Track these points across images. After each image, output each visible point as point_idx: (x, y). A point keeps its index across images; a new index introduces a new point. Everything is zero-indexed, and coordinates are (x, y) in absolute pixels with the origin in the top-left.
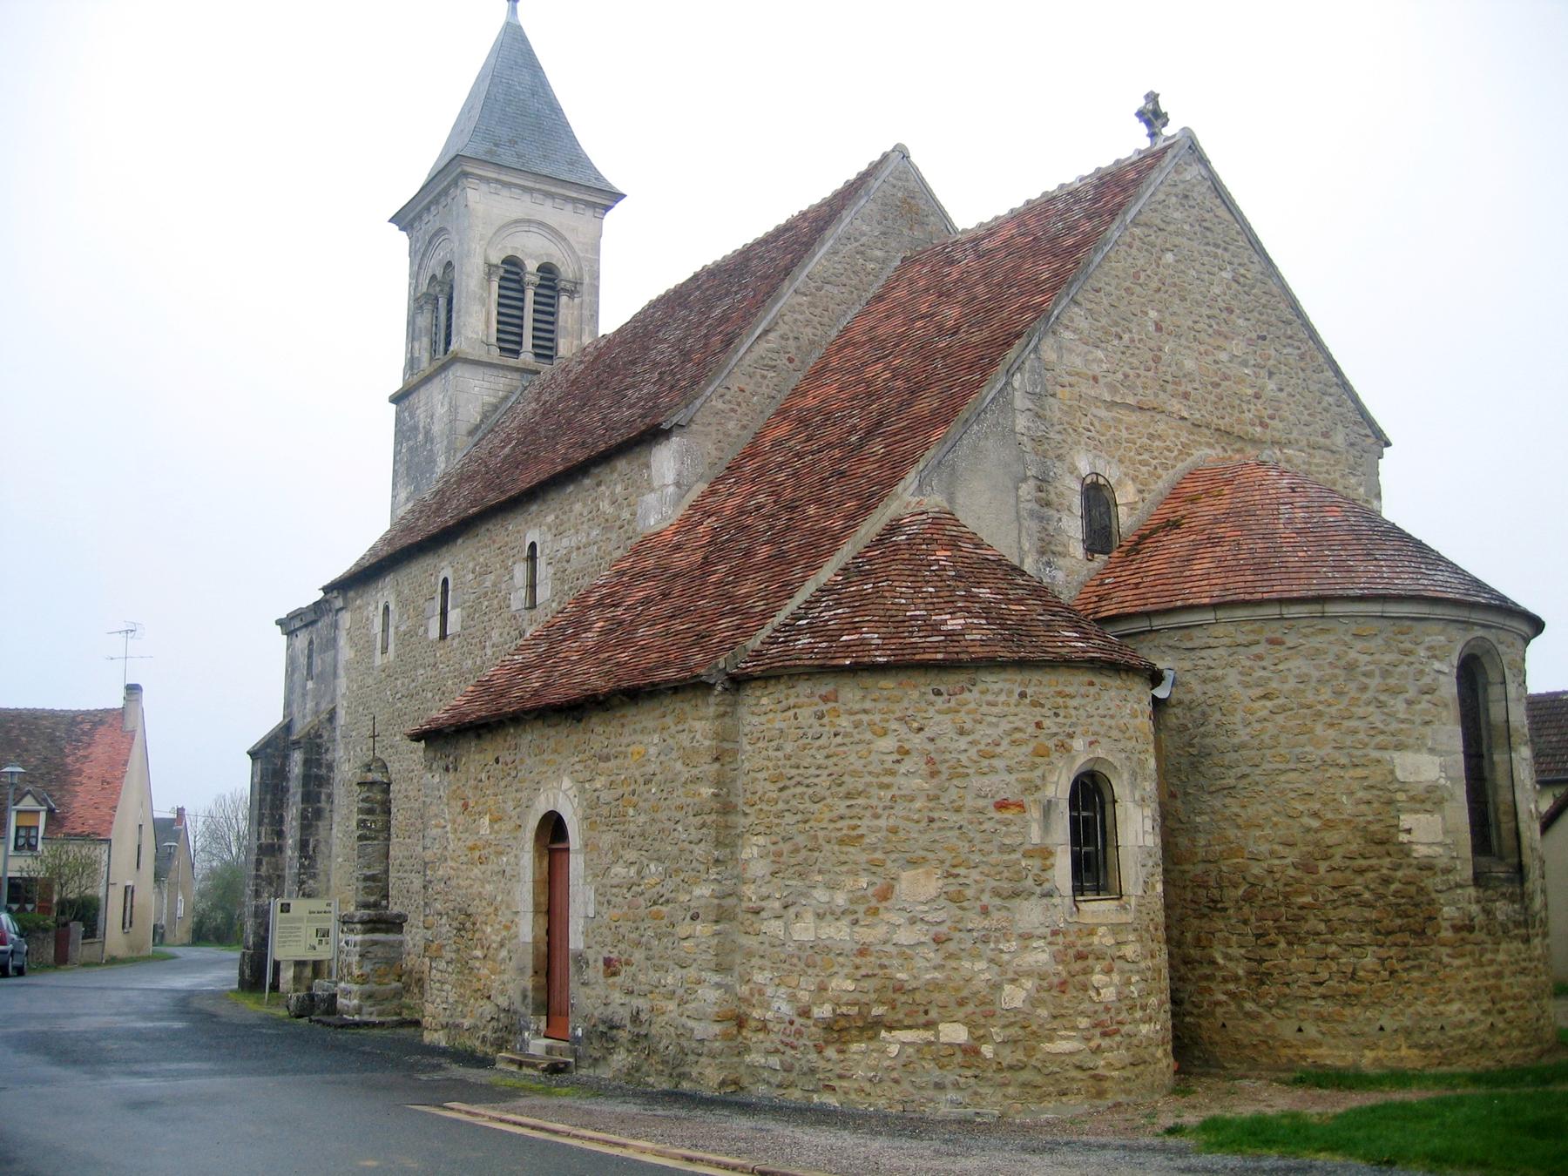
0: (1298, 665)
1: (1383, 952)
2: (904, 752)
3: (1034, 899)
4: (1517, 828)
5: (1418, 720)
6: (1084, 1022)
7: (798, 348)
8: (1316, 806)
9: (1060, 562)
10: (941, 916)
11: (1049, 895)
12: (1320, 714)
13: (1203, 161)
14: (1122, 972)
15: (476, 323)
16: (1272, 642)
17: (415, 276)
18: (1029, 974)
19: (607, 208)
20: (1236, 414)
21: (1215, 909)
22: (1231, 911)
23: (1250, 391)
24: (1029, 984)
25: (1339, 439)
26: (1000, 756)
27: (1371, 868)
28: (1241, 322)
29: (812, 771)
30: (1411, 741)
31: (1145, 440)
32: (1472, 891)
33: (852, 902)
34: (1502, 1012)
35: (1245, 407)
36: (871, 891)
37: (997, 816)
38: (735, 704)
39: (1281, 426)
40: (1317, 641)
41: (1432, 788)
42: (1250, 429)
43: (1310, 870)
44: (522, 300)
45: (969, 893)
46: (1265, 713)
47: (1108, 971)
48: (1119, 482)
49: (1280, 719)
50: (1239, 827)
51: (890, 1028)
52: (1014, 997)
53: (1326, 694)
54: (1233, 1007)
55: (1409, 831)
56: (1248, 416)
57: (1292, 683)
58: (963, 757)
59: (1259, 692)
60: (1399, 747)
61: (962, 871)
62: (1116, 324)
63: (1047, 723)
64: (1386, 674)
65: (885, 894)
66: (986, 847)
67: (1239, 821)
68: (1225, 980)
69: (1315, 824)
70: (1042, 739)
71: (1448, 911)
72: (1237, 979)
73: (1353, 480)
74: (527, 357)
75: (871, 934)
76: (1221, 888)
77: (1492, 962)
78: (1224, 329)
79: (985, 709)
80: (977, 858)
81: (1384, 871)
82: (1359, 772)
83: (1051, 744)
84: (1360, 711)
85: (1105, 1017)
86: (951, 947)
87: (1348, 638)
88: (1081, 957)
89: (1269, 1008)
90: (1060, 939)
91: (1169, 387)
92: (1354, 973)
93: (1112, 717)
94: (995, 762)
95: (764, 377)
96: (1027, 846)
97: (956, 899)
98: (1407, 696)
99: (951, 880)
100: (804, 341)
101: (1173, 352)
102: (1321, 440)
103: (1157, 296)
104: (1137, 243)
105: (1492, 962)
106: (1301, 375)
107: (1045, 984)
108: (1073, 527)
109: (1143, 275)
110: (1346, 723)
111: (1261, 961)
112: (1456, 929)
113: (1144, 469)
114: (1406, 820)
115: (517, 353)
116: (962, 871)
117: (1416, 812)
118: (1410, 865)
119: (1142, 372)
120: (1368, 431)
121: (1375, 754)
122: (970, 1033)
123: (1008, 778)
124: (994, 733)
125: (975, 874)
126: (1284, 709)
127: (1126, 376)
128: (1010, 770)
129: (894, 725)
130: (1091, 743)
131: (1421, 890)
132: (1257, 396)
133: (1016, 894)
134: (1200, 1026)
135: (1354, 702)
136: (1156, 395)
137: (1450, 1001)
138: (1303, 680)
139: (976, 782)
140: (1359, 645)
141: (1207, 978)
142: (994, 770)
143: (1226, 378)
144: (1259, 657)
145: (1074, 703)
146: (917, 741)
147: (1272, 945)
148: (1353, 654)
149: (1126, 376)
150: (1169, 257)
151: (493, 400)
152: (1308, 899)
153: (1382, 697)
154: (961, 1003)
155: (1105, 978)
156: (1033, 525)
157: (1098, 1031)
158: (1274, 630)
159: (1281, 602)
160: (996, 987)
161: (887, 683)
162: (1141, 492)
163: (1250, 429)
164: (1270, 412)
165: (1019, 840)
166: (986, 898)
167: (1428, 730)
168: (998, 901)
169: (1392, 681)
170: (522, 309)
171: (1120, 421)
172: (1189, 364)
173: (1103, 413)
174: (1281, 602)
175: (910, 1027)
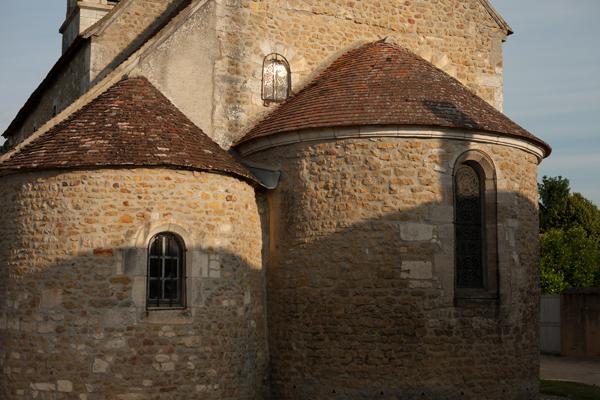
1: (386, 346)
3: (116, 307)
4: (498, 270)
6: (147, 383)
9: (244, 107)
11: (128, 305)
12: (352, 197)
14: (180, 353)
18: (109, 352)
21: (292, 316)
22: (300, 319)
24: (110, 359)
25: (471, 29)
26: (98, 222)
27: (381, 294)
29: (9, 231)
31: (317, 32)
32: (453, 310)
33: (20, 307)
34: (472, 385)
35: (397, 10)
36: (28, 302)
37: (95, 258)
41: (426, 245)
45: (76, 303)
47: (170, 352)
50: (307, 267)
51: (34, 382)
52: (101, 366)
54: (299, 377)
55: (408, 271)
56: (399, 16)
58: (76, 222)
65: (34, 303)
66: (87, 276)
67: (307, 263)
68: (297, 360)
69: (348, 266)
71: (432, 322)
72: (302, 359)
73: (480, 55)
75: (27, 328)
76: (296, 304)
77: (464, 355)
79: (92, 194)
80: (81, 282)
81: (389, 296)
82: (378, 234)
83: (134, 215)
85: (164, 379)
86: (65, 335)
88: (148, 343)
89: (317, 377)
90: (134, 332)
92: (367, 358)
93: (183, 198)
94: (95, 226)
95: (153, 6)
96: (113, 276)
98: (412, 186)
99: (67, 296)
105: (464, 355)
107: (121, 358)
111: (315, 349)
112: (438, 333)
113: (315, 51)
114: (406, 265)
116: (72, 290)
117: (414, 259)
118: (406, 293)
120: (497, 25)
121: (389, 223)
122: (74, 387)
123: (103, 235)
125: (80, 292)
130: (164, 215)
131: (413, 308)
133: (104, 304)
134: (283, 386)
137: (430, 378)
139: (83, 235)
141: (289, 358)
145: (149, 189)
147: (320, 340)
152: (339, 313)
153: (394, 187)
154: (69, 368)
155: (167, 357)
156: (225, 85)
157: (158, 388)
159: (334, 128)
162: (310, 64)
163: (401, 24)
164: (417, 13)
165: (107, 272)
166: (85, 307)
168: (93, 309)
173: (286, 17)
174: (334, 128)
175: (42, 381)
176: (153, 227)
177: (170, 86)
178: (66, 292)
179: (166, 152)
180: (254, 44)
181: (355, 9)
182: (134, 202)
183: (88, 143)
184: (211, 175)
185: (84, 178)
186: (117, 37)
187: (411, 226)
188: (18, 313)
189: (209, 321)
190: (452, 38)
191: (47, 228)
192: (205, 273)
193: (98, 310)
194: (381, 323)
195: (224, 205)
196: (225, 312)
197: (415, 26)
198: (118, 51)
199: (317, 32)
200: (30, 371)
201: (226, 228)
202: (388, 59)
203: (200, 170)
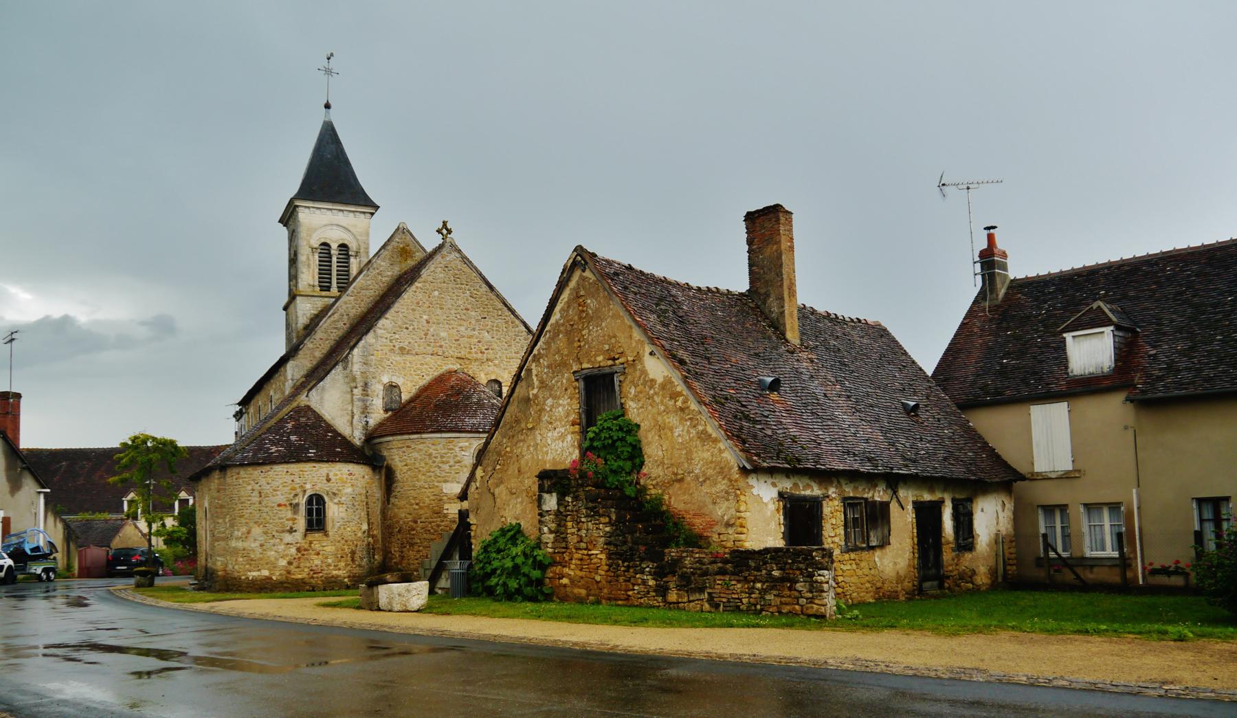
0: (415, 455)
13: (459, 251)
15: (309, 276)
19: (372, 214)
40: (421, 446)
43: (416, 522)
60: (446, 481)
74: (334, 290)
75: (246, 544)
97: (265, 533)
115: (328, 289)
146: (257, 487)
150: (436, 293)
156: (360, 404)
158: (409, 443)
160: (277, 559)
161: (250, 469)
172: (443, 334)
182: (297, 480)
183: (274, 449)
187: (448, 485)
201: (349, 490)
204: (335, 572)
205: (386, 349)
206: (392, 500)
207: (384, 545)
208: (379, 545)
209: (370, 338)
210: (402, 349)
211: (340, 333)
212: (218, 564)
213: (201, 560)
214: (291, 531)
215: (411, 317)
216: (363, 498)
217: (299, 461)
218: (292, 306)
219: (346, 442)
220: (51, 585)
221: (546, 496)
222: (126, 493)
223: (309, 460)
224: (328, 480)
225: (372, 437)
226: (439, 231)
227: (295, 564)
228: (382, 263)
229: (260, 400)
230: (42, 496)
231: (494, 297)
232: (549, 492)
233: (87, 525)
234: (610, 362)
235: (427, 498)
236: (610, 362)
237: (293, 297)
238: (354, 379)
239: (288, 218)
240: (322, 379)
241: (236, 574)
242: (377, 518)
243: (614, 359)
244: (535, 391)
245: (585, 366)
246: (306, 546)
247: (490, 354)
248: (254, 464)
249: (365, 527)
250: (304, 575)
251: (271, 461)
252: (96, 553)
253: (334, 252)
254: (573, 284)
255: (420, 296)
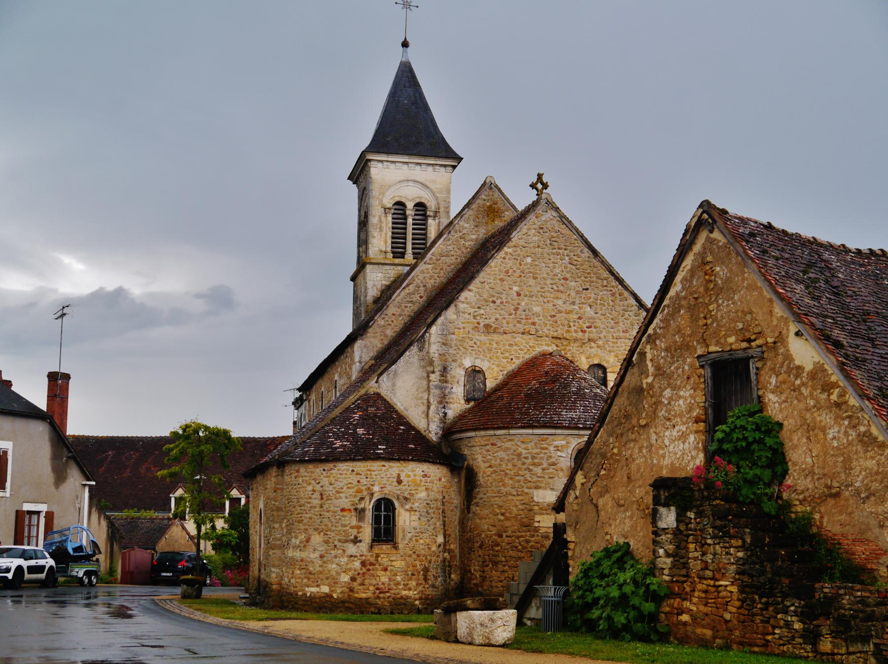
0: (501, 454)
2: (314, 491)
5: (547, 477)
7: (425, 291)
8: (503, 511)
9: (451, 406)
10: (322, 548)
11: (360, 541)
12: (506, 474)
13: (557, 209)
15: (380, 241)
16: (493, 444)
17: (359, 210)
18: (350, 570)
19: (454, 167)
20: (566, 328)
23: (577, 316)
27: (522, 536)
28: (573, 284)
30: (543, 485)
31: (507, 347)
35: (572, 324)
38: (283, 471)
39: (595, 330)
40: (508, 445)
42: (574, 335)
43: (501, 536)
44: (405, 224)
45: (331, 541)
46: (489, 473)
48: (489, 368)
49: (494, 475)
53: (510, 466)
55: (539, 522)
57: (498, 462)
59: (488, 464)
60: (537, 488)
61: (329, 533)
62: (494, 296)
63: (361, 481)
64: (533, 458)
65: (308, 541)
70: (360, 487)
74: (409, 257)
75: (304, 555)
78: (561, 288)
80: (333, 528)
82: (521, 498)
83: (363, 488)
84: (521, 473)
85: (382, 586)
86: (325, 559)
87: (519, 443)
91: (523, 321)
95: (406, 307)
97: (326, 542)
100: (429, 286)
101: (527, 304)
102: (621, 334)
103: (519, 279)
104: (509, 256)
106: (611, 303)
108: (458, 391)
109: (511, 271)
110: (517, 478)
113: (505, 361)
114: (537, 518)
115: (402, 255)
116: (329, 533)
119: (506, 316)
121: (526, 490)
123: (346, 500)
124: (341, 484)
125: (333, 534)
126: (495, 472)
127: (496, 319)
128: (346, 498)
129: (313, 482)
132: (580, 318)
133: (346, 541)
135: (520, 469)
136: (515, 326)
138: (502, 460)
139: (334, 501)
140: (523, 446)
142: (341, 498)
143: (560, 312)
144: (488, 451)
145: (373, 473)
146: (318, 487)
147: (487, 566)
148: (520, 450)
149: (496, 319)
150: (529, 260)
151: (388, 283)
153: (531, 467)
154: (327, 578)
156: (437, 392)
157: (378, 592)
158: (494, 440)
160: (338, 574)
161: (311, 467)
163: (574, 335)
164: (588, 325)
165: (348, 522)
166: (336, 543)
167: (551, 480)
169: (536, 461)
170: (405, 229)
171: (492, 340)
172: (537, 309)
176: (375, 495)
177: (398, 395)
178: (325, 534)
179: (383, 449)
180: (459, 361)
181: (537, 327)
182: (364, 481)
183: (338, 443)
184: (411, 463)
185: (335, 466)
186: (379, 334)
188: (299, 546)
189: (410, 552)
190: (619, 341)
191: (314, 496)
192: (407, 523)
193: (345, 545)
194: (522, 555)
195: (421, 481)
196: (422, 547)
197: (587, 335)
198: (380, 345)
199: (507, 347)
200: (305, 580)
201: (423, 495)
202: (547, 373)
203: (404, 460)
204: (404, 593)
205: (469, 327)
206: (473, 508)
207: (462, 562)
208: (457, 562)
209: (450, 314)
210: (487, 326)
211: (416, 308)
212: (273, 575)
213: (254, 570)
214: (356, 541)
215: (499, 288)
216: (439, 504)
217: (366, 458)
218: (361, 276)
219: (419, 437)
220: (93, 591)
221: (662, 510)
222: (174, 489)
223: (378, 458)
224: (399, 482)
225: (450, 431)
226: (533, 186)
227: (359, 580)
228: (465, 225)
229: (323, 386)
230: (87, 489)
231: (598, 264)
232: (667, 505)
233: (133, 523)
234: (744, 345)
235: (515, 507)
236: (744, 345)
237: (362, 265)
238: (431, 363)
239: (359, 174)
240: (394, 362)
241: (292, 589)
242: (454, 530)
243: (749, 341)
244: (650, 380)
245: (713, 348)
246: (372, 560)
247: (593, 333)
248: (316, 460)
249: (440, 539)
250: (369, 594)
251: (335, 457)
252: (140, 556)
253: (410, 212)
254: (697, 247)
255: (510, 263)
